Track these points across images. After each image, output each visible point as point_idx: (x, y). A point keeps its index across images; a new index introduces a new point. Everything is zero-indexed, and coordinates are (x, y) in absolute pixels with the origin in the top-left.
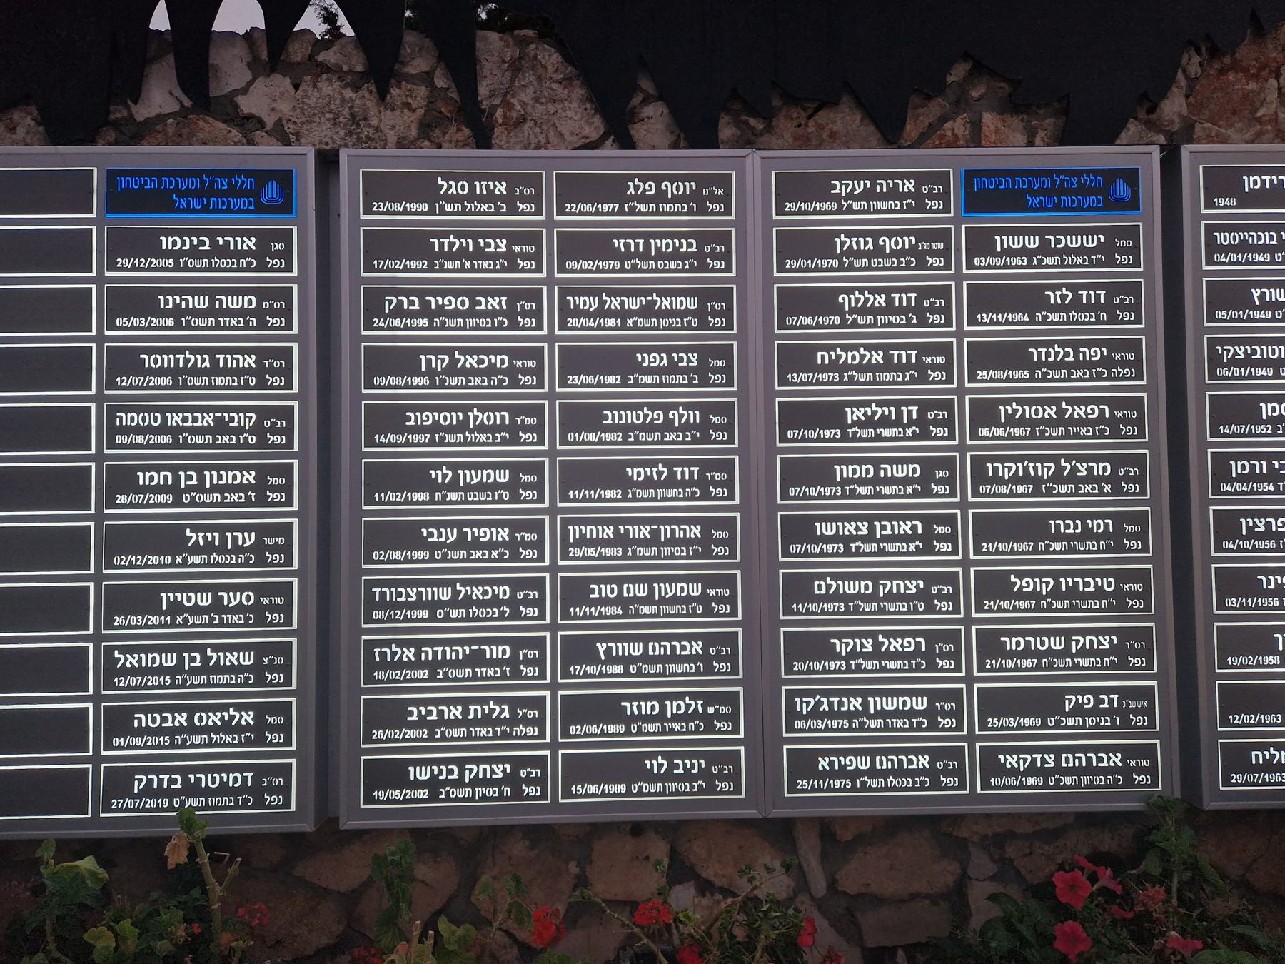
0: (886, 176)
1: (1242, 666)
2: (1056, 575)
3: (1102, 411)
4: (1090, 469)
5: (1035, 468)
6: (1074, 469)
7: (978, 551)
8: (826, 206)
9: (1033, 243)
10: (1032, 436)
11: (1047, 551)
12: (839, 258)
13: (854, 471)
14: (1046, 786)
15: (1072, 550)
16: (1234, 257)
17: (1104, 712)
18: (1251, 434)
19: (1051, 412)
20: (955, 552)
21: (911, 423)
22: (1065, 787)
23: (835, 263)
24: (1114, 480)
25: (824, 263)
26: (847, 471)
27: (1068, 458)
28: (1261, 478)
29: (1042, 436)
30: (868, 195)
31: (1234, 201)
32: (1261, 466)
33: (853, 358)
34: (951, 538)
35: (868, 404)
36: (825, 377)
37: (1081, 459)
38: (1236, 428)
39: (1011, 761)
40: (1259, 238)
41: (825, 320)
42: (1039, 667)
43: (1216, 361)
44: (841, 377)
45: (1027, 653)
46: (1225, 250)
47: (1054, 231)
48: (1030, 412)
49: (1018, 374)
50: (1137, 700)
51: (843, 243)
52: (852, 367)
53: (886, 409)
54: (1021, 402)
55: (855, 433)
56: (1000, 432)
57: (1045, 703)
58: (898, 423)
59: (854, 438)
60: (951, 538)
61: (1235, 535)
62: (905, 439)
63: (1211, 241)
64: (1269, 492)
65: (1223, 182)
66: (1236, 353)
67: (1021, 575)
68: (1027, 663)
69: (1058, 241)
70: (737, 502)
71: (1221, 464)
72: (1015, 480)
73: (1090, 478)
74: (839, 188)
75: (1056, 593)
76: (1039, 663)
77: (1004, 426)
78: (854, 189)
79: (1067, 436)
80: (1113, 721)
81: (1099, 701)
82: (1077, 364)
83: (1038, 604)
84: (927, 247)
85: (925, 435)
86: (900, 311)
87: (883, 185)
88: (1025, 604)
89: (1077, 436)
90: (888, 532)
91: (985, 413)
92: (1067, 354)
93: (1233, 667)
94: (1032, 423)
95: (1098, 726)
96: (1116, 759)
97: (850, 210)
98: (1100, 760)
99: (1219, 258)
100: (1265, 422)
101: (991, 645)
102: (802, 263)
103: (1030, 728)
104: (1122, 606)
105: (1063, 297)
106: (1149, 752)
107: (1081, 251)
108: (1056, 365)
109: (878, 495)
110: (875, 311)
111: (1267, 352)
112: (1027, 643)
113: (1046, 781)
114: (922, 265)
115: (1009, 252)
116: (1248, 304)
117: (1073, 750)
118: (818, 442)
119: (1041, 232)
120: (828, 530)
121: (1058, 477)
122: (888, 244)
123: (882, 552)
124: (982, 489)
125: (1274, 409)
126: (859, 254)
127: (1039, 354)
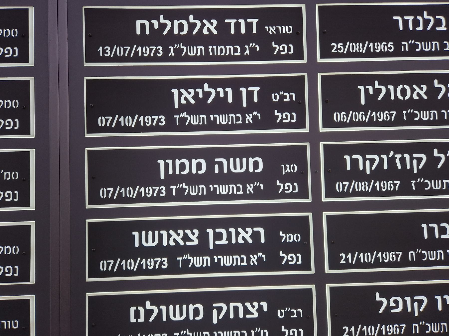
5: (403, 161)
10: (399, 121)
11: (419, 263)
13: (182, 167)
19: (421, 91)
20: (306, 265)
21: (252, 106)
26: (174, 166)
33: (181, 27)
34: (302, 248)
35: (199, 84)
36: (146, 51)
48: (395, 92)
49: (381, 47)
52: (179, 39)
53: (221, 90)
55: (183, 120)
56: (360, 116)
58: (236, 107)
59: (183, 126)
60: (302, 248)
62: (244, 126)
67: (387, 292)
77: (365, 109)
85: (269, 121)
90: (224, 241)
91: (341, 93)
92: (438, 23)
94: (398, 105)
108: (426, 36)
109: (212, 196)
118: (137, 132)
120: (149, 240)
123: (216, 267)
124: (339, 187)
127: (406, 22)
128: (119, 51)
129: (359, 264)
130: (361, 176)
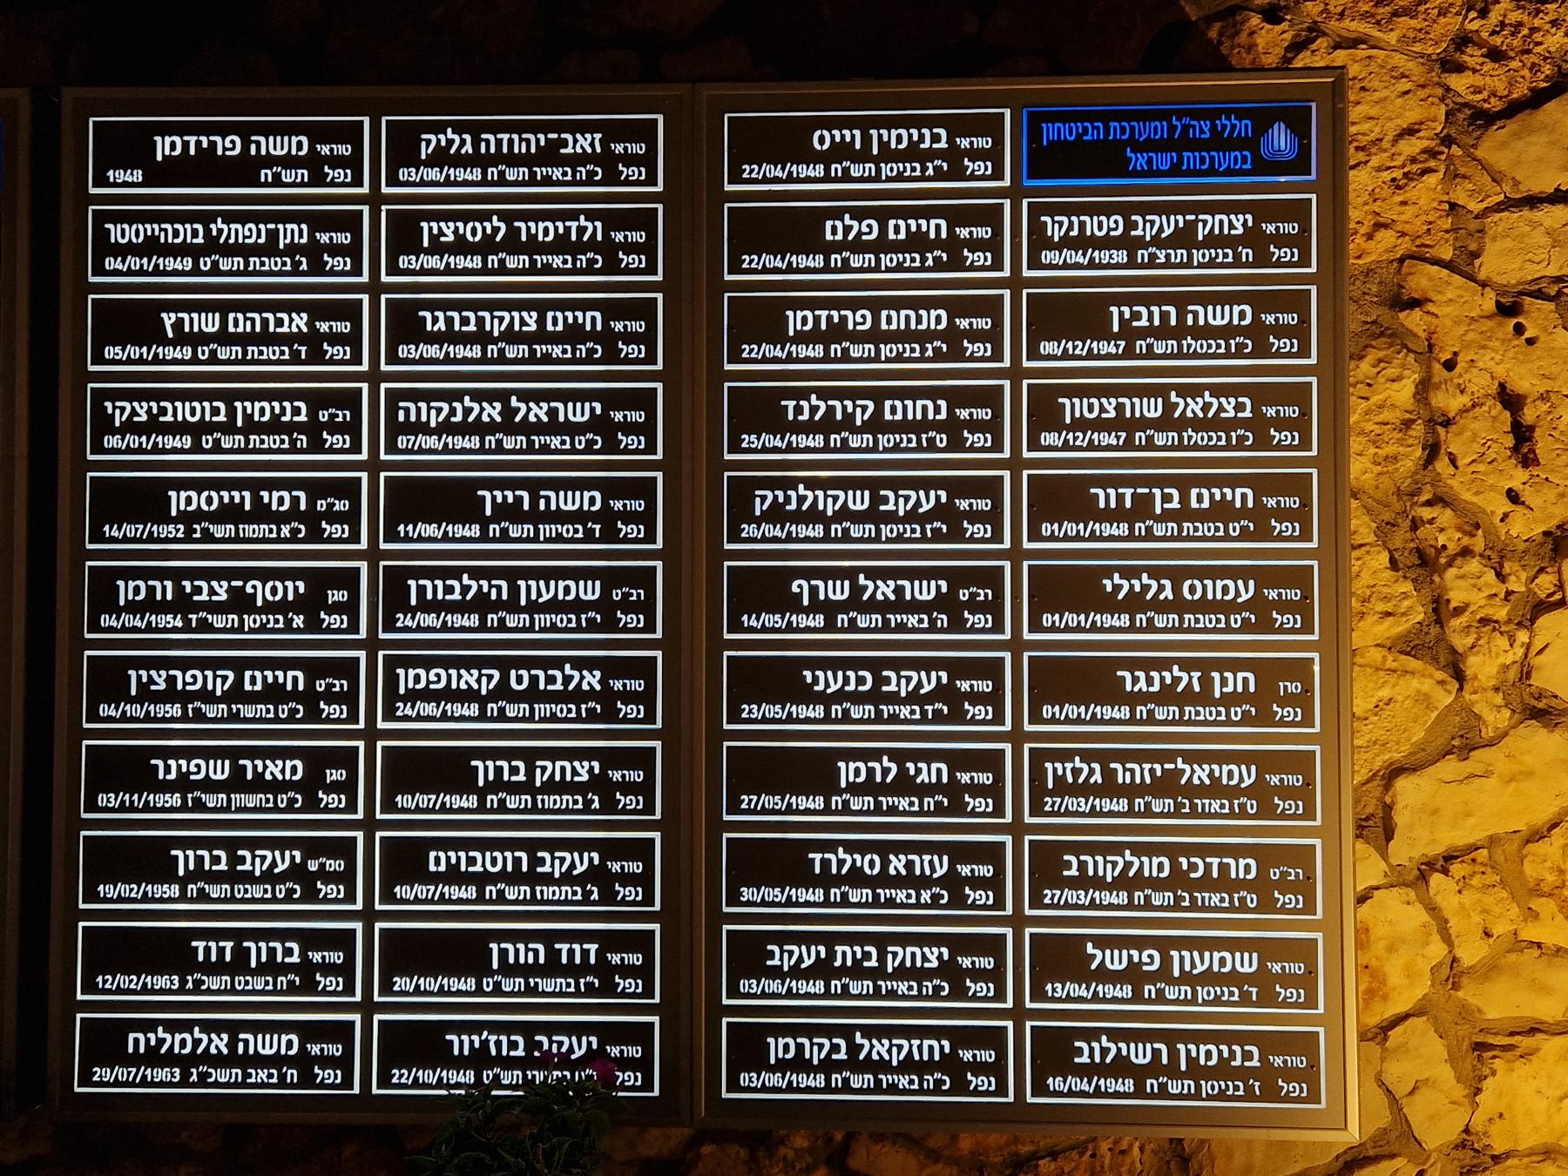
1: (120, 900)
16: (134, 262)
18: (151, 539)
28: (163, 607)
31: (138, 176)
32: (164, 588)
38: (129, 530)
40: (176, 234)
43: (104, 425)
46: (123, 251)
61: (119, 693)
65: (129, 148)
66: (134, 413)
71: (105, 583)
93: (106, 900)
99: (111, 263)
100: (175, 521)
111: (182, 411)
125: (189, 501)
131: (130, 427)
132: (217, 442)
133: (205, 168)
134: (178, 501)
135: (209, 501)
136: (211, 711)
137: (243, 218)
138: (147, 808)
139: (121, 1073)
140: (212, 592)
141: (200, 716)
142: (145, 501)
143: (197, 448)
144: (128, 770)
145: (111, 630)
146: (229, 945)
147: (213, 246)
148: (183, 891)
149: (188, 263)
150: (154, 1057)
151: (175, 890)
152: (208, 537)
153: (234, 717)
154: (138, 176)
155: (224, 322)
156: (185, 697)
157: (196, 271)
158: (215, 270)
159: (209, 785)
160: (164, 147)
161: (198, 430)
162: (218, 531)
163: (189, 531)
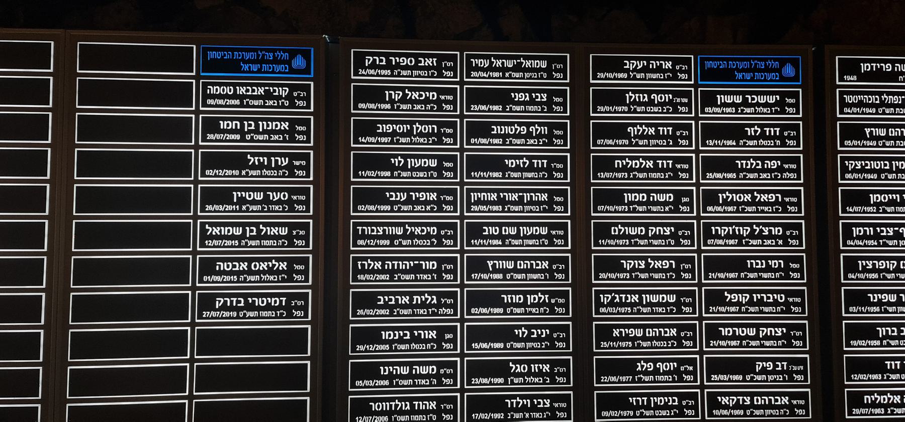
0: (655, 59)
1: (859, 346)
2: (751, 292)
3: (777, 198)
4: (770, 231)
5: (739, 230)
6: (761, 231)
7: (706, 278)
8: (621, 75)
9: (738, 100)
10: (737, 211)
12: (628, 106)
14: (745, 415)
15: (760, 278)
16: (855, 110)
17: (778, 373)
18: (864, 212)
19: (748, 197)
22: (756, 416)
23: (626, 109)
24: (784, 237)
25: (620, 109)
27: (758, 225)
28: (869, 238)
29: (743, 211)
30: (645, 70)
31: (855, 78)
33: (636, 164)
36: (620, 175)
37: (765, 225)
38: (856, 209)
39: (725, 400)
40: (869, 99)
41: (620, 142)
42: (741, 346)
43: (845, 170)
44: (629, 175)
45: (734, 337)
46: (850, 106)
47: (751, 93)
48: (736, 197)
49: (730, 175)
50: (797, 365)
51: (630, 97)
52: (635, 170)
54: (731, 192)
56: (719, 209)
57: (745, 367)
61: (855, 270)
63: (842, 100)
64: (874, 246)
66: (856, 165)
68: (734, 343)
69: (753, 99)
70: (569, 248)
71: (848, 228)
72: (728, 236)
73: (770, 236)
74: (629, 65)
75: (751, 303)
76: (741, 343)
77: (722, 205)
78: (637, 66)
79: (757, 212)
80: (784, 378)
81: (776, 366)
82: (764, 170)
83: (740, 309)
84: (678, 100)
86: (663, 137)
87: (654, 64)
88: (733, 309)
89: (763, 212)
92: (757, 164)
93: (854, 347)
94: (737, 204)
95: (775, 381)
96: (785, 400)
97: (635, 78)
98: (776, 400)
99: (846, 110)
100: (873, 205)
101: (713, 333)
102: (607, 108)
103: (736, 381)
104: (789, 311)
105: (756, 131)
106: (804, 396)
107: (766, 105)
110: (649, 137)
111: (874, 165)
112: (734, 332)
113: (745, 412)
114: (676, 111)
115: (725, 105)
116: (863, 137)
117: (761, 394)
119: (743, 94)
121: (752, 236)
122: (657, 98)
124: (709, 242)
125: (877, 198)
126: (640, 104)
127: (742, 164)
128: (607, 175)
129: (718, 279)
130: (719, 237)
131: (855, 171)
132: (886, 176)
133: (879, 75)
134: (873, 198)
135: (885, 198)
136: (889, 276)
137: (893, 94)
138: (867, 312)
139: (863, 411)
140: (887, 232)
141: (885, 278)
142: (859, 198)
143: (879, 179)
144: (859, 298)
145: (851, 246)
146: (898, 363)
147: (883, 104)
148: (881, 343)
149: (874, 110)
150: (874, 405)
151: (878, 343)
152: (885, 212)
153: (897, 278)
154: (855, 78)
155: (887, 132)
156: (879, 271)
157: (877, 113)
158: (884, 113)
159: (889, 304)
160: (865, 67)
161: (879, 172)
162: (889, 209)
163: (878, 209)
